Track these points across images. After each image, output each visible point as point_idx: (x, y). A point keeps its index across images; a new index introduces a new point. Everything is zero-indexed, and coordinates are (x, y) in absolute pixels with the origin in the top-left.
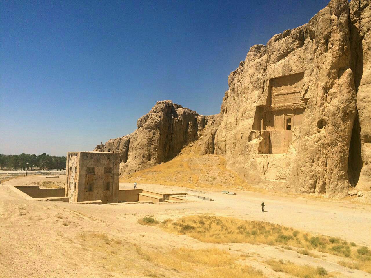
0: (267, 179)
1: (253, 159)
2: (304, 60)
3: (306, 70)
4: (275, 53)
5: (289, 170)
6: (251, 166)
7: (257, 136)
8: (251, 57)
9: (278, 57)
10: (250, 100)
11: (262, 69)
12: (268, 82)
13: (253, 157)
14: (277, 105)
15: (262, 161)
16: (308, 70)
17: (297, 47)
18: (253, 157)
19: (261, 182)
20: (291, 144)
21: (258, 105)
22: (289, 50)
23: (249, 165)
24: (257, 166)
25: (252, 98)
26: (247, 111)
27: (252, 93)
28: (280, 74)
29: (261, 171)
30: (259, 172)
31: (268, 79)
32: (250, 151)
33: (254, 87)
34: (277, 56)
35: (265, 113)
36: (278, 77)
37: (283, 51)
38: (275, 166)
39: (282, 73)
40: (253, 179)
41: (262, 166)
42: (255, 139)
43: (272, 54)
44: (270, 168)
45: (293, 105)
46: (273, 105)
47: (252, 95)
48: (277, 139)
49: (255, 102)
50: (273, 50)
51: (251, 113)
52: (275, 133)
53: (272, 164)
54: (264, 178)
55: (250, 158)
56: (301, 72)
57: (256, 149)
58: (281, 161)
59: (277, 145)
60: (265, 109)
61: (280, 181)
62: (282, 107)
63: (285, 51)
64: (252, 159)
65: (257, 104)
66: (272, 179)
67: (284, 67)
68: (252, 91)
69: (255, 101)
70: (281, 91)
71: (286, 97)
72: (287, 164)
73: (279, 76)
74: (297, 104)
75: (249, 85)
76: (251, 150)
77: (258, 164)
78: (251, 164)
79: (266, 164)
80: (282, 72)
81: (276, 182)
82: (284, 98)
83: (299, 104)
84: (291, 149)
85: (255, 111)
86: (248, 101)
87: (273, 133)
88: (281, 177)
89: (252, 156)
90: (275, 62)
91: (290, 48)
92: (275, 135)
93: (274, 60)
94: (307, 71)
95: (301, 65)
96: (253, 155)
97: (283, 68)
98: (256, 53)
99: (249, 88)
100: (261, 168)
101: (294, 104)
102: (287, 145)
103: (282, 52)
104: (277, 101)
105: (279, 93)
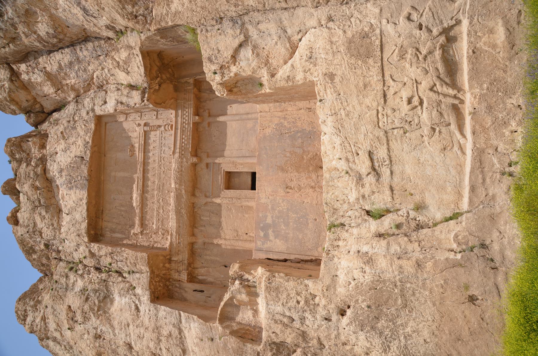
0: (465, 205)
1: (343, 313)
2: (72, 119)
3: (93, 110)
4: (40, 225)
5: (389, 29)
6: (381, 334)
7: (244, 297)
8: (38, 320)
9: (47, 212)
10: (132, 334)
11: (67, 277)
12: (95, 247)
13: (334, 317)
14: (172, 224)
15: (354, 249)
16: (94, 104)
17: (43, 146)
18: (334, 317)
19: (483, 246)
20: (273, 76)
21: (148, 293)
22: (39, 170)
23: (377, 341)
24: (384, 281)
25: (128, 325)
26: (158, 351)
27: (115, 323)
28: (81, 200)
29: (410, 247)
30: (419, 265)
31: (90, 251)
32: (304, 335)
33: (98, 310)
34: (44, 213)
35: (192, 278)
36: (89, 204)
37: (37, 188)
38: (381, 153)
39: (82, 188)
40: (468, 309)
41: (383, 243)
42: (256, 312)
43: (41, 233)
44: (392, 189)
45: (177, 155)
46: (169, 237)
47: (120, 323)
48: (287, 224)
49: (137, 308)
50: (31, 230)
51: (165, 333)
52: (262, 234)
53: (372, 179)
54: (458, 228)
55: (338, 336)
56: (93, 126)
57: (293, 294)
58: (347, 115)
59: (311, 225)
60: (176, 276)
61: (466, 87)
62: (178, 197)
63: (37, 183)
64: (345, 320)
65: (145, 298)
66: (460, 167)
67: (71, 184)
68: (109, 320)
69: (133, 307)
70: (134, 205)
71: (154, 182)
72: (359, 56)
73: (85, 201)
74: (179, 138)
75: (93, 332)
76: (297, 324)
77: (368, 278)
78: (373, 328)
79: (373, 225)
80: (78, 191)
81: (474, 114)
82: (156, 192)
83: (179, 131)
84: (292, 65)
85: (163, 310)
86: (133, 343)
87: (263, 244)
88: (438, 88)
89: (328, 319)
90: (58, 223)
91: (37, 166)
92: (270, 232)
93: (53, 225)
94: (96, 108)
95: (79, 129)
96: (321, 312)
97: (70, 189)
98: (33, 300)
99: (100, 337)
100: (395, 248)
101: (178, 150)
102: (314, 177)
103: (38, 192)
104: (160, 223)
105: (137, 211)
